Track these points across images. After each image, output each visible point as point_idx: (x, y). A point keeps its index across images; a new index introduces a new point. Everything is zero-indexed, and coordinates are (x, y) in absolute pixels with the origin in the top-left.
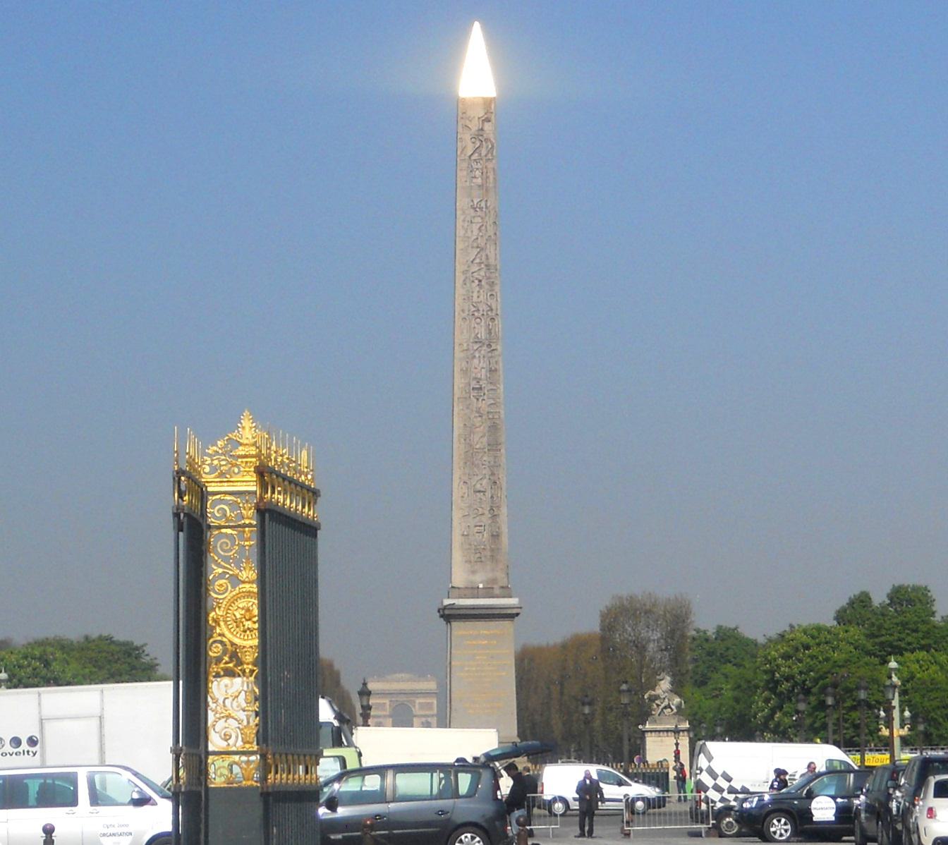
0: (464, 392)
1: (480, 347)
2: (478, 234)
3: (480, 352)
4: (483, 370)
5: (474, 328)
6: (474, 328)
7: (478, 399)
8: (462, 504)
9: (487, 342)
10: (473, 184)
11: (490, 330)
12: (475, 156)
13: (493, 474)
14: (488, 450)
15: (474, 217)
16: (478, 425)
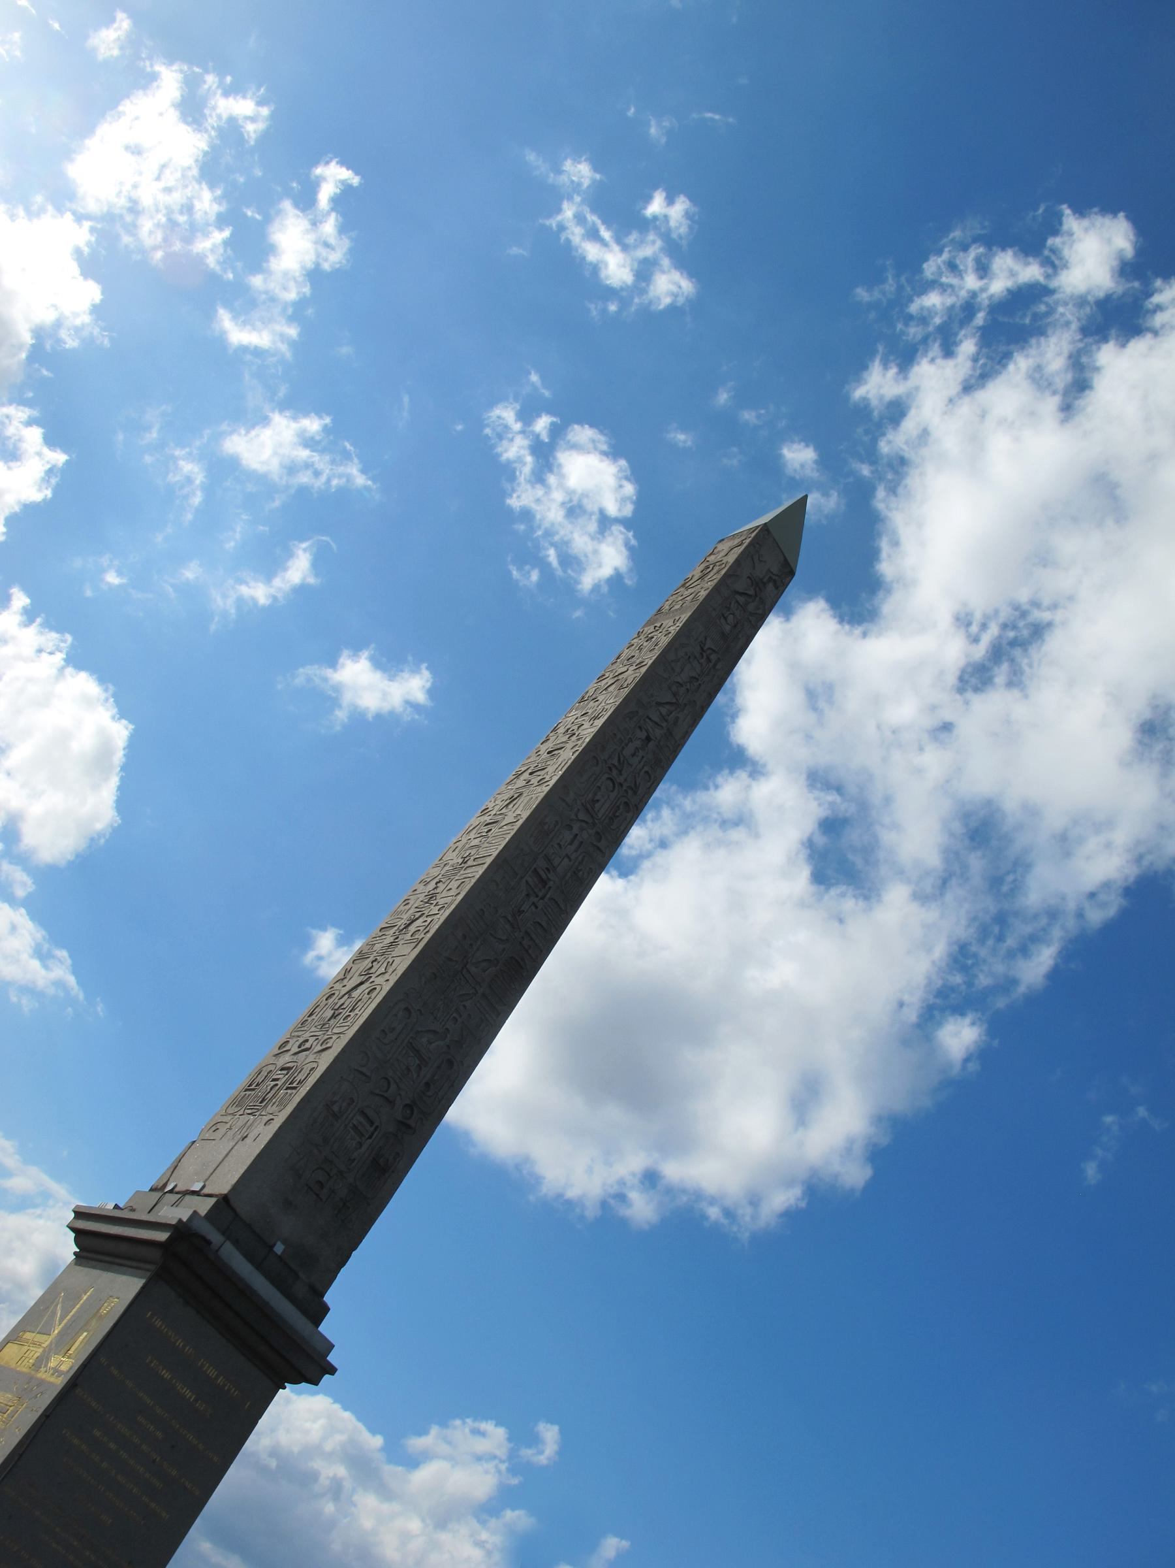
1: (587, 823)
3: (582, 829)
4: (566, 860)
5: (599, 788)
12: (741, 599)
14: (484, 995)
15: (695, 657)
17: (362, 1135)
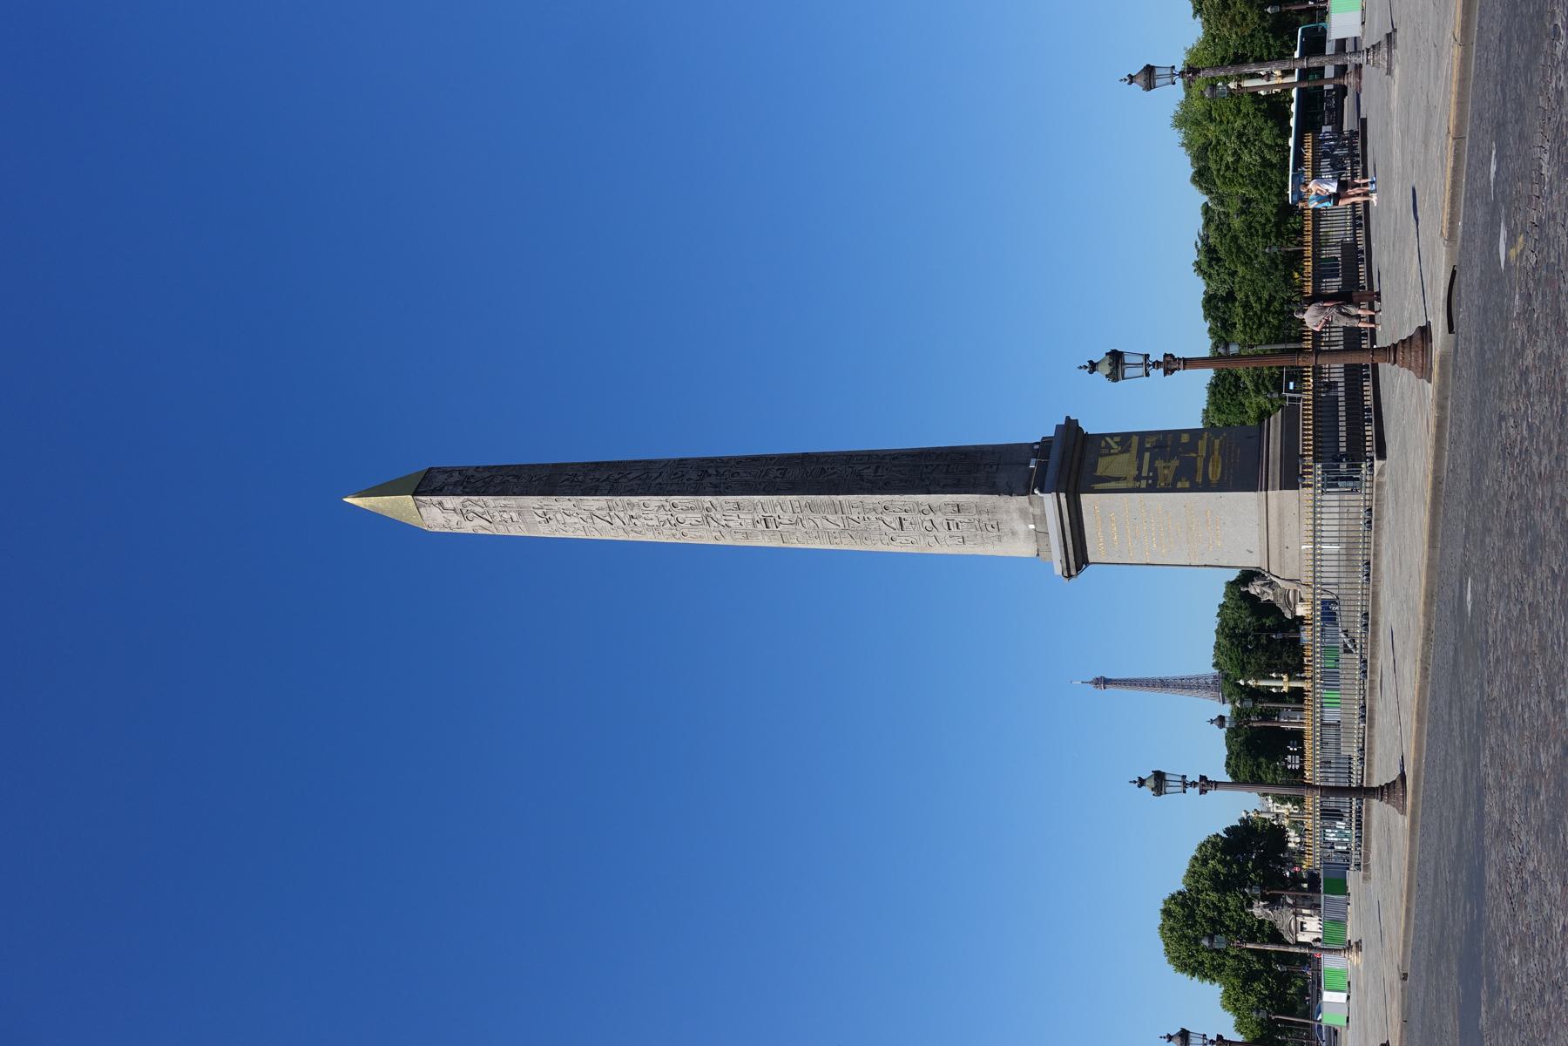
0: (776, 537)
8: (922, 542)
9: (705, 513)
16: (812, 523)
17: (957, 524)
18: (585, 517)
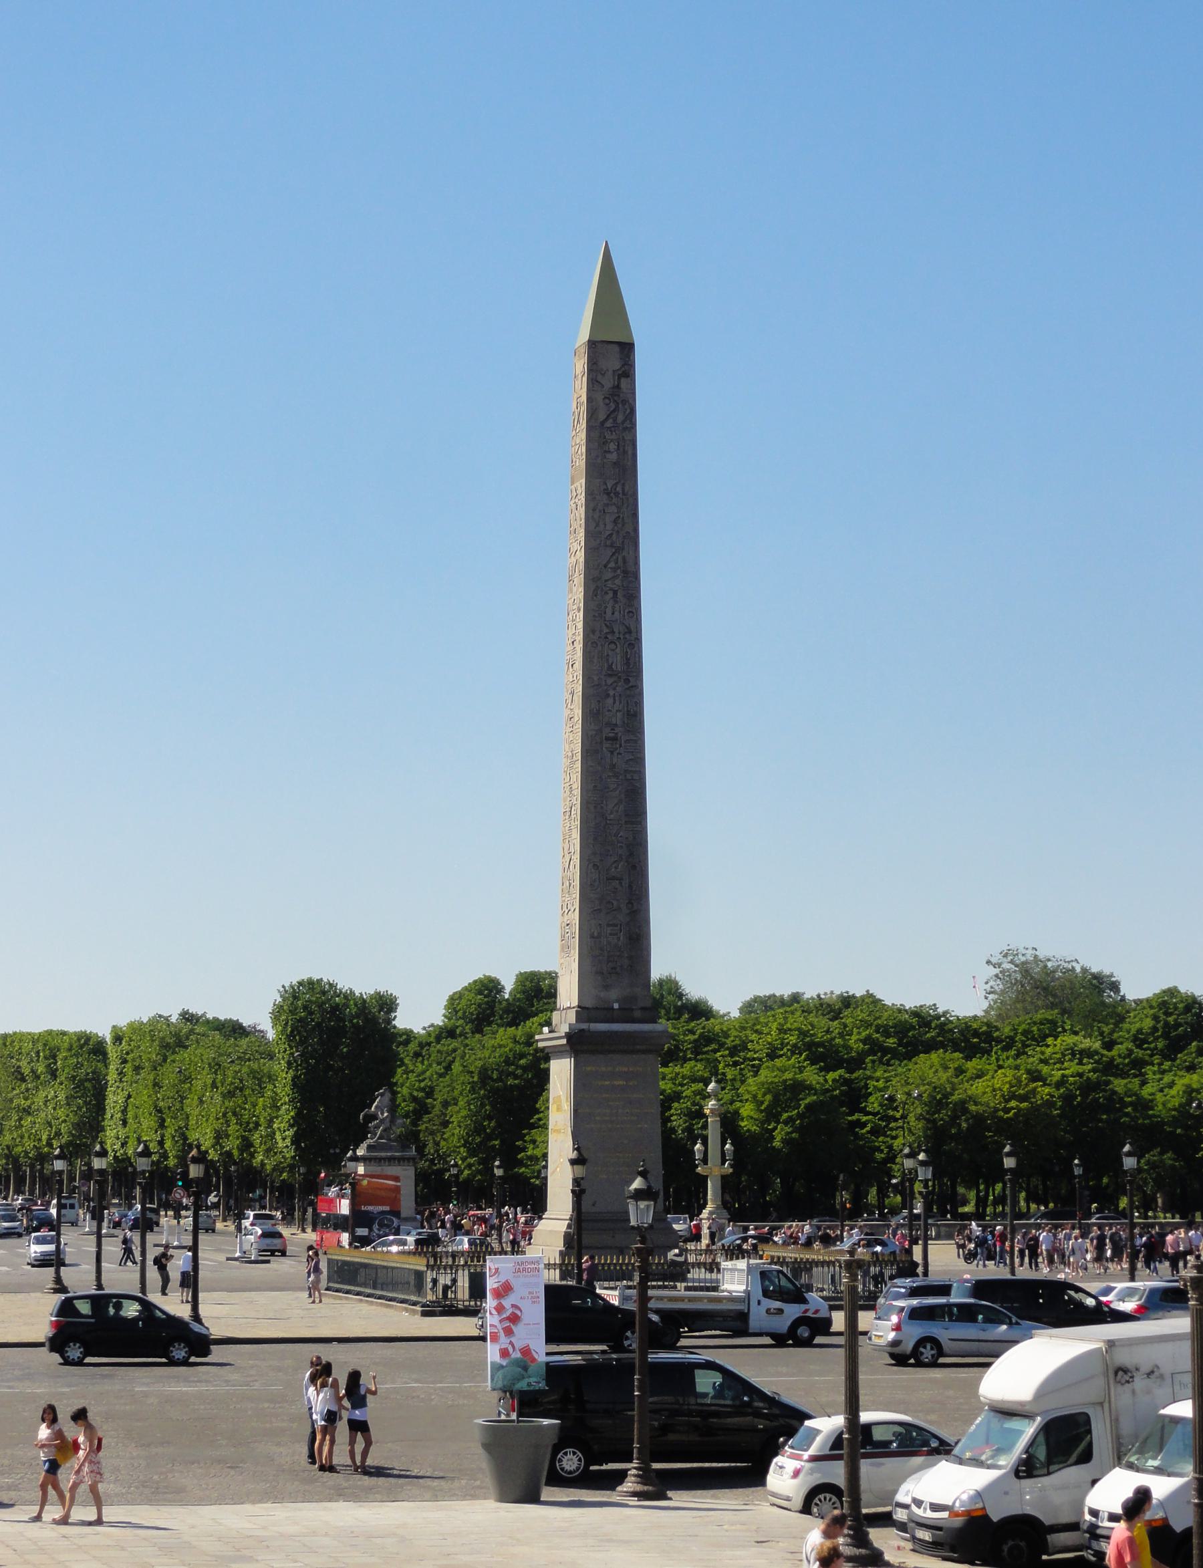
1: (615, 682)
2: (613, 530)
3: (614, 689)
5: (608, 655)
6: (608, 655)
7: (612, 753)
8: (592, 895)
10: (605, 461)
11: (628, 659)
12: (609, 424)
13: (631, 854)
16: (612, 786)
17: (617, 934)
18: (614, 536)
